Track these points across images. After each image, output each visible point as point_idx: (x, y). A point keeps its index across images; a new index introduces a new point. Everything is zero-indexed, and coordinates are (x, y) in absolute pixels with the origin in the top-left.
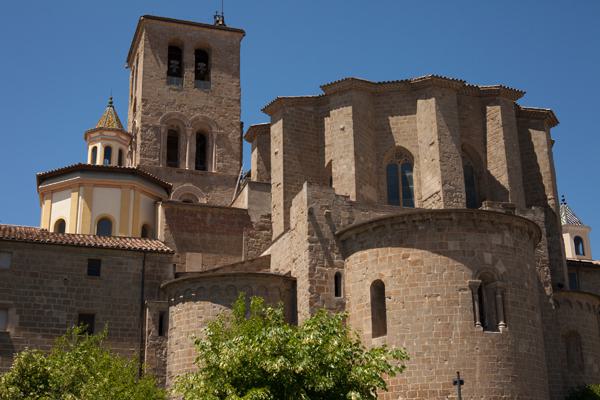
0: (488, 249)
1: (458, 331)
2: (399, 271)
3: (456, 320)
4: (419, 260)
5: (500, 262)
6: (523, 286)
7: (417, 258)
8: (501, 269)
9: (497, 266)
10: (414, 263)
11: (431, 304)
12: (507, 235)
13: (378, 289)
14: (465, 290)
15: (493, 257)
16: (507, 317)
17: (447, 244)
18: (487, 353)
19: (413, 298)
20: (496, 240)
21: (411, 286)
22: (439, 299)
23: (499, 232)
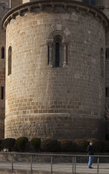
0: (59, 22)
1: (39, 68)
2: (16, 40)
3: (38, 62)
4: (23, 33)
5: (66, 29)
6: (82, 43)
7: (23, 31)
8: (67, 33)
9: (64, 32)
10: (22, 34)
11: (28, 54)
12: (74, 14)
13: (10, 48)
14: (44, 46)
15: (62, 26)
16: (68, 60)
17: (37, 22)
18: (53, 78)
19: (20, 53)
20: (65, 17)
21: (20, 46)
22: (31, 51)
23: (68, 13)
